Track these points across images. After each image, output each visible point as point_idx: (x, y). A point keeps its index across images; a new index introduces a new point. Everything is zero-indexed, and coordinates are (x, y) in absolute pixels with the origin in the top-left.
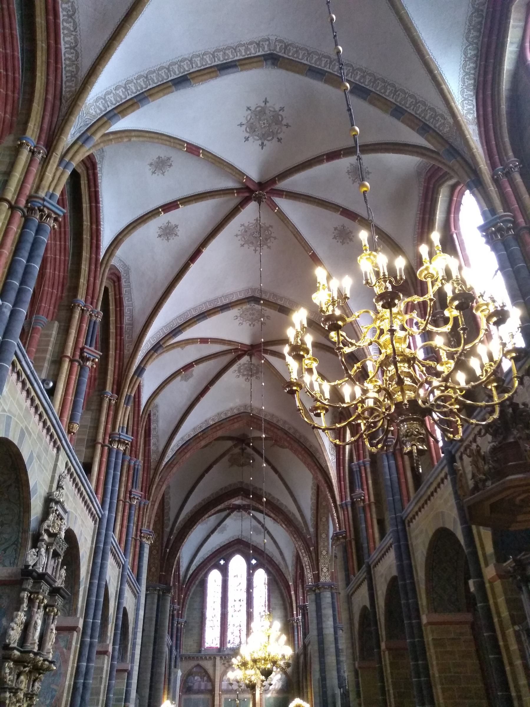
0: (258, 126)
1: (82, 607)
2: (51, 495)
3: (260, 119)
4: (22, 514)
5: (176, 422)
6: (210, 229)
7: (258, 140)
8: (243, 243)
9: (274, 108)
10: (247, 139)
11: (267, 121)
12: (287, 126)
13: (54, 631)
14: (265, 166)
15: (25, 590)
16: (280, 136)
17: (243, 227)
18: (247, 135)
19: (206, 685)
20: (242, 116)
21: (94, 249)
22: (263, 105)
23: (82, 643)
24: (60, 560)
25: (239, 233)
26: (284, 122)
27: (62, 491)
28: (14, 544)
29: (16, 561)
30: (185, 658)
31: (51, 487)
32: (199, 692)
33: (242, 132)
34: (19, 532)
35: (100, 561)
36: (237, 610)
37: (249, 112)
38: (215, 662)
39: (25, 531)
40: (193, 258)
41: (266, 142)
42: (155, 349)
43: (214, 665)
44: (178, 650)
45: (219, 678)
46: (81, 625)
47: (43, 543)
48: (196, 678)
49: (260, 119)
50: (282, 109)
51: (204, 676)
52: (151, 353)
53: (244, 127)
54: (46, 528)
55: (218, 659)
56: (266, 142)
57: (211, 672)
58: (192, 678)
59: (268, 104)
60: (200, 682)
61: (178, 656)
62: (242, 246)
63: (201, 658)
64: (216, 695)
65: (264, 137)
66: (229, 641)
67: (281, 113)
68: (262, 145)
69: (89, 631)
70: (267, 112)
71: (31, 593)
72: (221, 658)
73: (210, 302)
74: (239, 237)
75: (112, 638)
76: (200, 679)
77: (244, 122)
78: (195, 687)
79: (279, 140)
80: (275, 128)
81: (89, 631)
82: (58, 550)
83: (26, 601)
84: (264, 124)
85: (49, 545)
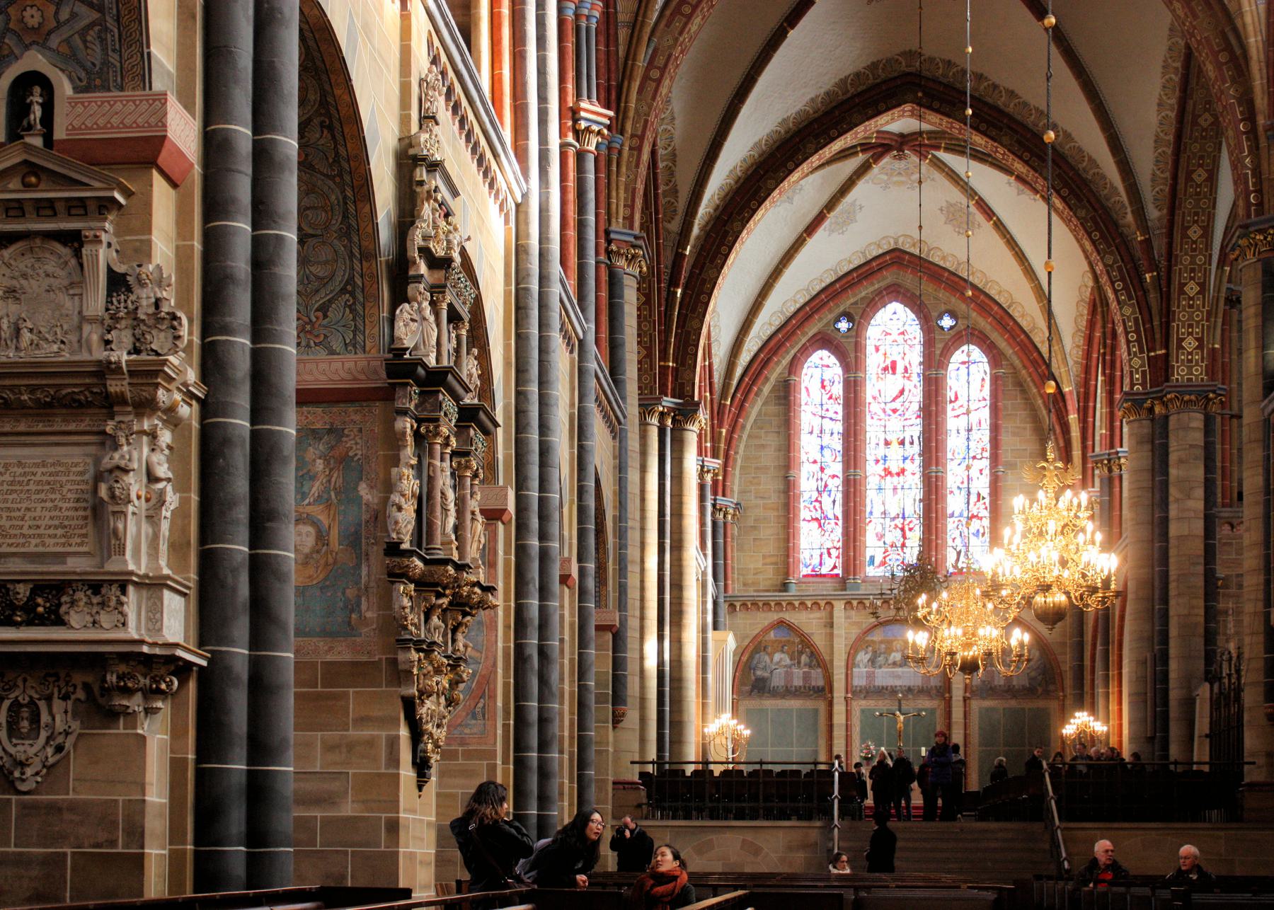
1: (506, 457)
2: (411, 146)
4: (352, 208)
13: (480, 518)
15: (404, 412)
19: (806, 677)
23: (522, 551)
24: (464, 332)
27: (436, 129)
28: (343, 291)
29: (360, 338)
30: (744, 605)
31: (405, 120)
32: (789, 692)
34: (352, 255)
35: (536, 331)
36: (894, 470)
38: (831, 616)
39: (370, 254)
45: (844, 657)
46: (511, 507)
47: (421, 286)
48: (777, 657)
51: (801, 653)
54: (422, 243)
55: (839, 606)
57: (819, 640)
58: (767, 658)
60: (790, 667)
61: (721, 600)
63: (790, 604)
66: (872, 558)
69: (534, 522)
71: (420, 421)
72: (849, 603)
75: (575, 541)
76: (788, 661)
78: (777, 681)
81: (534, 522)
82: (457, 307)
83: (410, 439)
85: (437, 290)
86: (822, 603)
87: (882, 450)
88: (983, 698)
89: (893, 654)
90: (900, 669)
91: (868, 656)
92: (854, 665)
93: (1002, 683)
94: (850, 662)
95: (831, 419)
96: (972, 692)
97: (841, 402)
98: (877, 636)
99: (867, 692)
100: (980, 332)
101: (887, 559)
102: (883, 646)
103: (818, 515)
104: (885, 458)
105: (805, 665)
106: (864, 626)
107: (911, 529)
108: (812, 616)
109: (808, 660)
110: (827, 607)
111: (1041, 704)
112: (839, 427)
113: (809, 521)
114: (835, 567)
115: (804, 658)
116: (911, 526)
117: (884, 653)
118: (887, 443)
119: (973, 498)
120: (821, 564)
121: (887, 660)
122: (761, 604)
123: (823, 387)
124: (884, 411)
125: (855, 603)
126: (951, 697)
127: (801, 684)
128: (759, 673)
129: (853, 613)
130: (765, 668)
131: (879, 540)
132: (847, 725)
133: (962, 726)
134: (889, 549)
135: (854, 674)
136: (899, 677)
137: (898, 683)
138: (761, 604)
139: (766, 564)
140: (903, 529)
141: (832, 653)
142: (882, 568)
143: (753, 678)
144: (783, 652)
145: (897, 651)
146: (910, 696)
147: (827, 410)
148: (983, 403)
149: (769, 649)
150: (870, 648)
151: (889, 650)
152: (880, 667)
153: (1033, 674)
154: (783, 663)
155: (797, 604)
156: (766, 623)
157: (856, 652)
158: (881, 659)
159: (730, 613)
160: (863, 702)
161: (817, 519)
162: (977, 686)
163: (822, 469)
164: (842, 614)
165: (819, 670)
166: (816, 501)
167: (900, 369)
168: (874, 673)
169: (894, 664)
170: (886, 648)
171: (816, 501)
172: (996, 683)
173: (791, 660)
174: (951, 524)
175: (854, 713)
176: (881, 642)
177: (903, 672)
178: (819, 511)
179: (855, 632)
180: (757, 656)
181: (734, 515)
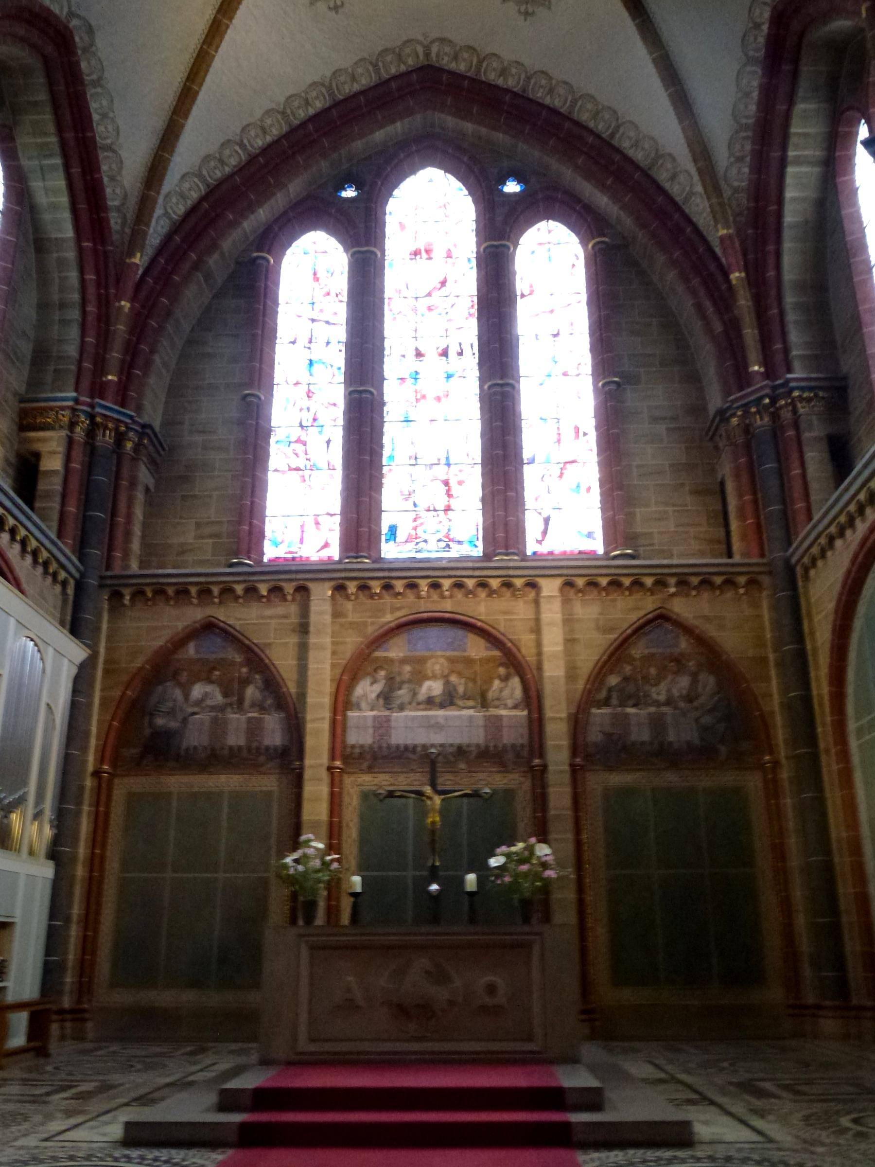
19: (254, 729)
30: (139, 593)
38: (305, 612)
43: (304, 629)
44: (95, 553)
45: (328, 688)
48: (197, 691)
51: (245, 682)
58: (178, 693)
60: (222, 709)
61: (93, 582)
63: (227, 591)
64: (308, 774)
66: (393, 529)
72: (340, 588)
76: (218, 698)
86: (289, 588)
87: (412, 364)
88: (610, 769)
89: (427, 684)
90: (441, 713)
91: (378, 688)
92: (348, 705)
93: (646, 736)
94: (341, 699)
95: (327, 322)
96: (588, 757)
97: (345, 299)
98: (396, 650)
99: (375, 758)
100: (567, 192)
101: (420, 531)
102: (407, 668)
103: (301, 462)
104: (416, 376)
105: (253, 705)
106: (370, 630)
107: (460, 483)
108: (269, 612)
109: (258, 695)
110: (298, 597)
111: (728, 778)
112: (340, 333)
113: (283, 472)
114: (326, 545)
115: (251, 692)
116: (460, 478)
117: (409, 681)
118: (419, 354)
119: (568, 433)
120: (302, 541)
121: (415, 694)
122: (170, 591)
123: (316, 279)
124: (415, 310)
125: (352, 587)
126: (545, 767)
127: (242, 741)
128: (160, 721)
129: (349, 606)
130: (172, 713)
131: (406, 499)
132: (331, 824)
133: (570, 825)
134: (423, 514)
135: (350, 723)
136: (438, 727)
137: (438, 738)
138: (170, 591)
139: (201, 537)
140: (446, 483)
141: (302, 682)
142: (411, 546)
143: (147, 732)
144: (211, 682)
145: (434, 677)
146: (462, 766)
147: (321, 311)
148: (578, 297)
149: (184, 677)
150: (382, 673)
151: (419, 677)
152: (402, 708)
153: (707, 720)
154: (209, 702)
155: (239, 589)
156: (180, 625)
157: (354, 679)
158: (403, 693)
159: (112, 610)
160: (366, 778)
161: (298, 469)
162: (596, 744)
163: (309, 394)
164: (327, 607)
165: (283, 715)
166: (298, 441)
167: (438, 253)
168: (388, 719)
169: (430, 702)
170: (412, 673)
171: (298, 441)
172: (634, 737)
173: (225, 695)
174: (530, 474)
175: (346, 799)
176: (404, 661)
177: (446, 718)
178: (302, 456)
179: (352, 642)
180: (160, 688)
181: (137, 447)
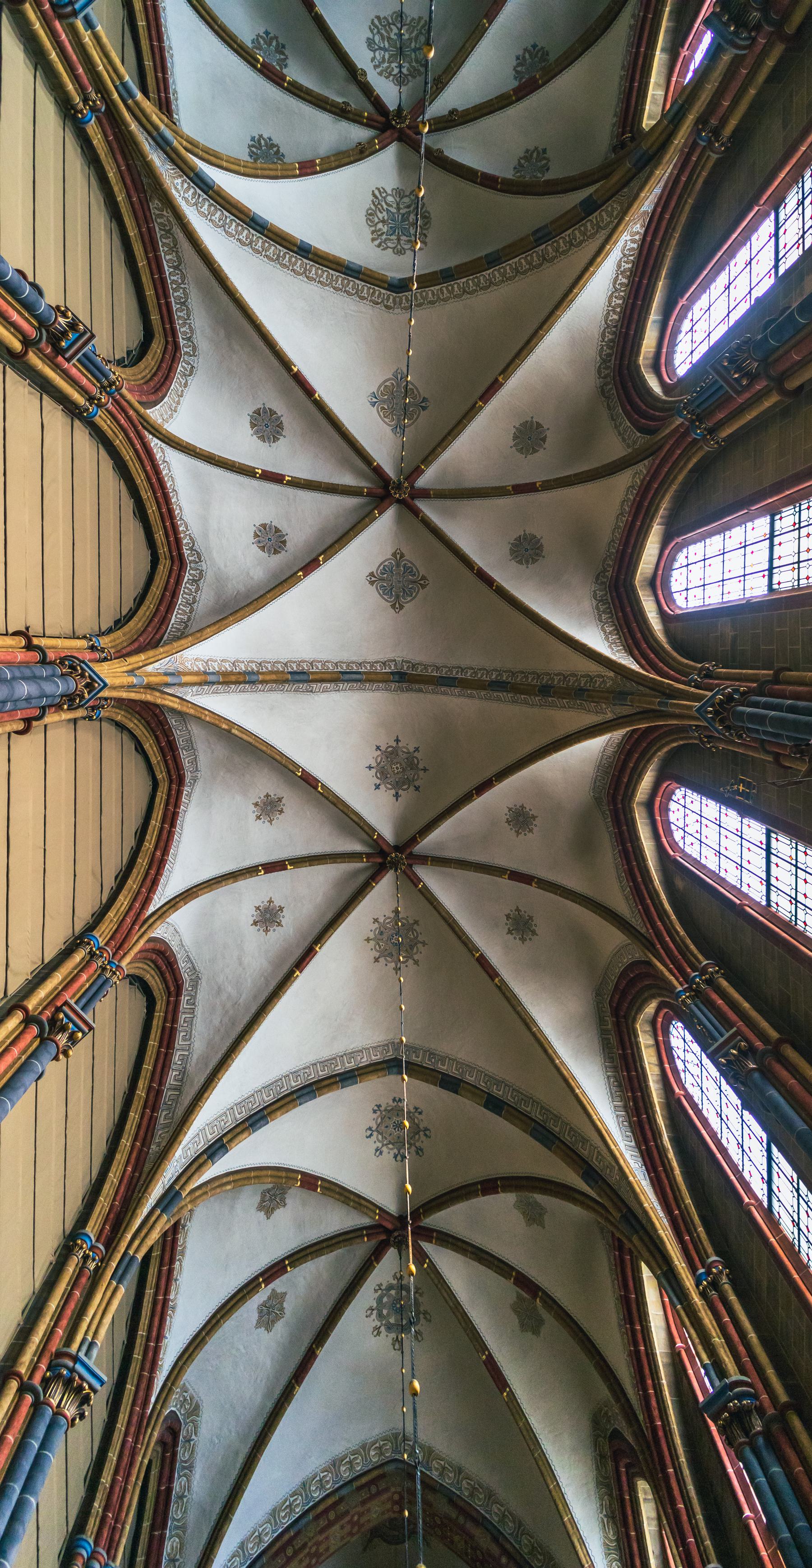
0: (390, 771)
3: (392, 763)
5: (234, 1474)
6: (329, 916)
7: (391, 789)
8: (377, 954)
9: (407, 749)
10: (377, 787)
11: (401, 765)
12: (425, 770)
14: (401, 824)
16: (417, 783)
17: (376, 925)
18: (378, 782)
20: (371, 757)
21: (148, 882)
22: (394, 744)
25: (372, 936)
26: (421, 766)
33: (371, 778)
37: (379, 753)
40: (301, 963)
41: (400, 792)
42: (209, 1152)
49: (392, 763)
50: (417, 749)
52: (201, 1161)
53: (374, 771)
56: (400, 792)
59: (400, 744)
62: (376, 960)
65: (398, 786)
67: (416, 754)
68: (397, 796)
70: (400, 753)
73: (324, 1063)
74: (372, 943)
77: (374, 764)
79: (417, 789)
80: (410, 773)
84: (397, 768)
